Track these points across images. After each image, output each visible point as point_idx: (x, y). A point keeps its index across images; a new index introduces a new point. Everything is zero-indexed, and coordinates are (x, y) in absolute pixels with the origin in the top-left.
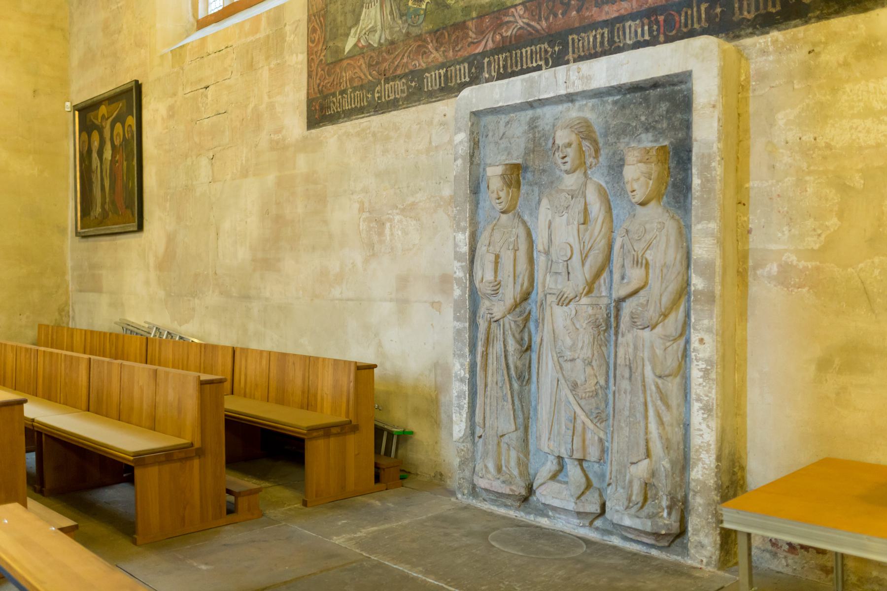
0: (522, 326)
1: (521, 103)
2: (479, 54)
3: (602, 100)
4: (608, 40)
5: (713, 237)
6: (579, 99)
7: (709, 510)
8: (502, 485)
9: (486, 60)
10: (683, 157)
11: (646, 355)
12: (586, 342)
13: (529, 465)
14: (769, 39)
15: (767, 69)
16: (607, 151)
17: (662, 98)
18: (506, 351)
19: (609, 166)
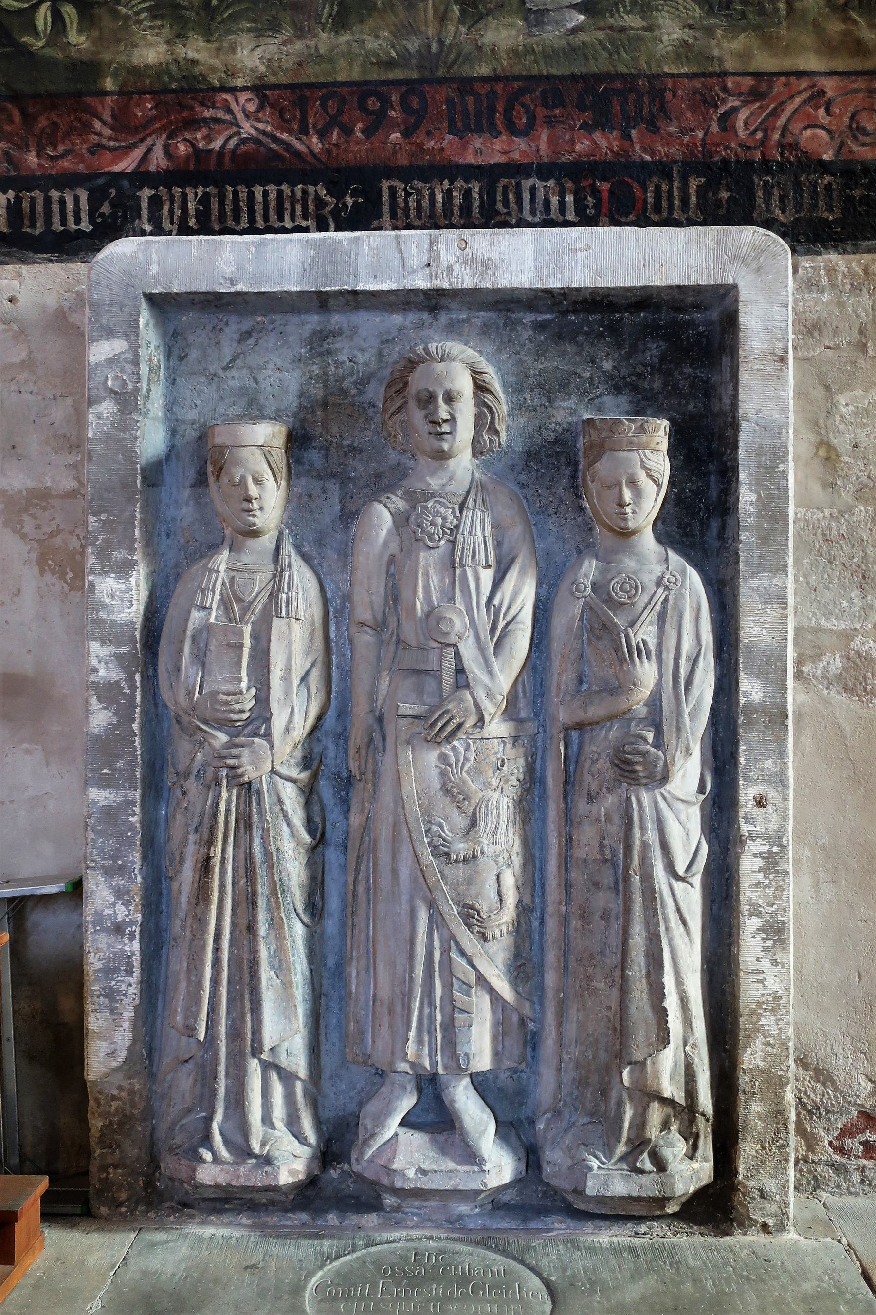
1: (302, 292)
2: (122, 175)
3: (509, 318)
4: (482, 206)
9: (146, 193)
10: (698, 449)
13: (320, 1098)
14: (822, 264)
17: (651, 330)
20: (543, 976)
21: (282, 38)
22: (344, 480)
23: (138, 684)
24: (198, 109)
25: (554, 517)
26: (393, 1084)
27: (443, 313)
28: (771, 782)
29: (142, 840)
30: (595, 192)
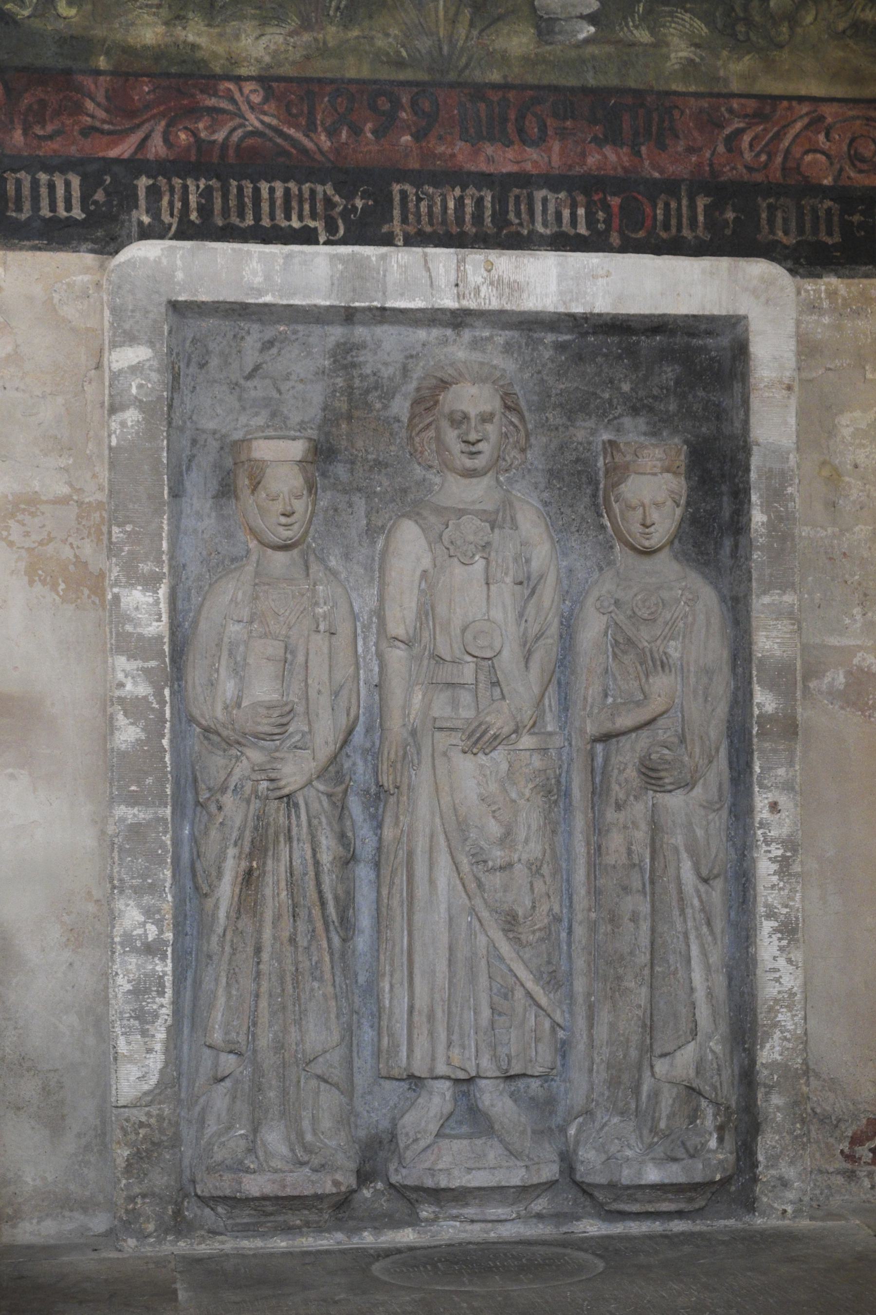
0: (339, 804)
2: (117, 161)
3: (529, 337)
4: (493, 215)
5: (791, 619)
6: (476, 324)
7: (795, 1114)
8: (314, 1177)
11: (679, 840)
12: (534, 827)
14: (823, 288)
15: (820, 337)
16: (544, 440)
17: (666, 355)
18: (317, 863)
19: (550, 472)
20: (571, 984)
21: (288, 28)
22: (370, 495)
23: (168, 698)
24: (199, 97)
25: (577, 535)
26: (431, 1093)
27: (467, 331)
28: (784, 789)
29: (173, 858)
30: (606, 207)
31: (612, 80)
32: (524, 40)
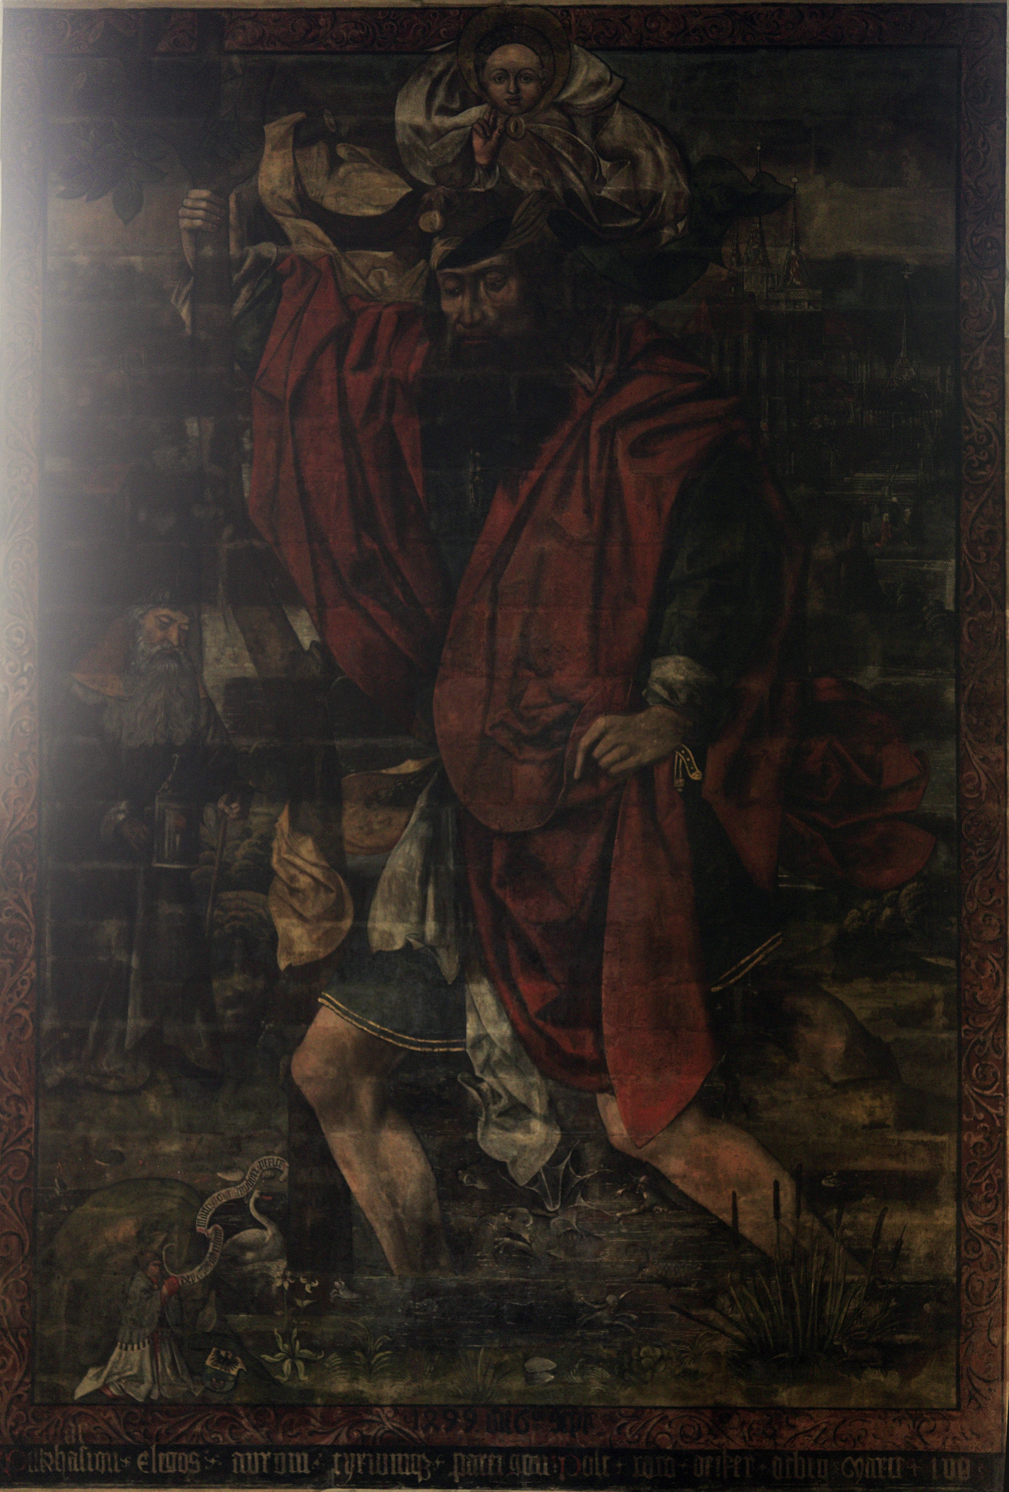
2: (325, 1446)
4: (503, 1467)
30: (558, 1462)
31: (560, 1401)
32: (519, 1383)
